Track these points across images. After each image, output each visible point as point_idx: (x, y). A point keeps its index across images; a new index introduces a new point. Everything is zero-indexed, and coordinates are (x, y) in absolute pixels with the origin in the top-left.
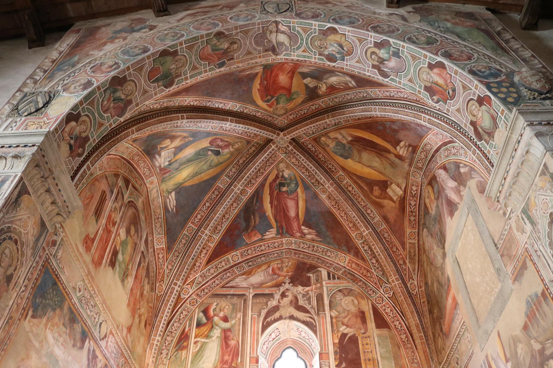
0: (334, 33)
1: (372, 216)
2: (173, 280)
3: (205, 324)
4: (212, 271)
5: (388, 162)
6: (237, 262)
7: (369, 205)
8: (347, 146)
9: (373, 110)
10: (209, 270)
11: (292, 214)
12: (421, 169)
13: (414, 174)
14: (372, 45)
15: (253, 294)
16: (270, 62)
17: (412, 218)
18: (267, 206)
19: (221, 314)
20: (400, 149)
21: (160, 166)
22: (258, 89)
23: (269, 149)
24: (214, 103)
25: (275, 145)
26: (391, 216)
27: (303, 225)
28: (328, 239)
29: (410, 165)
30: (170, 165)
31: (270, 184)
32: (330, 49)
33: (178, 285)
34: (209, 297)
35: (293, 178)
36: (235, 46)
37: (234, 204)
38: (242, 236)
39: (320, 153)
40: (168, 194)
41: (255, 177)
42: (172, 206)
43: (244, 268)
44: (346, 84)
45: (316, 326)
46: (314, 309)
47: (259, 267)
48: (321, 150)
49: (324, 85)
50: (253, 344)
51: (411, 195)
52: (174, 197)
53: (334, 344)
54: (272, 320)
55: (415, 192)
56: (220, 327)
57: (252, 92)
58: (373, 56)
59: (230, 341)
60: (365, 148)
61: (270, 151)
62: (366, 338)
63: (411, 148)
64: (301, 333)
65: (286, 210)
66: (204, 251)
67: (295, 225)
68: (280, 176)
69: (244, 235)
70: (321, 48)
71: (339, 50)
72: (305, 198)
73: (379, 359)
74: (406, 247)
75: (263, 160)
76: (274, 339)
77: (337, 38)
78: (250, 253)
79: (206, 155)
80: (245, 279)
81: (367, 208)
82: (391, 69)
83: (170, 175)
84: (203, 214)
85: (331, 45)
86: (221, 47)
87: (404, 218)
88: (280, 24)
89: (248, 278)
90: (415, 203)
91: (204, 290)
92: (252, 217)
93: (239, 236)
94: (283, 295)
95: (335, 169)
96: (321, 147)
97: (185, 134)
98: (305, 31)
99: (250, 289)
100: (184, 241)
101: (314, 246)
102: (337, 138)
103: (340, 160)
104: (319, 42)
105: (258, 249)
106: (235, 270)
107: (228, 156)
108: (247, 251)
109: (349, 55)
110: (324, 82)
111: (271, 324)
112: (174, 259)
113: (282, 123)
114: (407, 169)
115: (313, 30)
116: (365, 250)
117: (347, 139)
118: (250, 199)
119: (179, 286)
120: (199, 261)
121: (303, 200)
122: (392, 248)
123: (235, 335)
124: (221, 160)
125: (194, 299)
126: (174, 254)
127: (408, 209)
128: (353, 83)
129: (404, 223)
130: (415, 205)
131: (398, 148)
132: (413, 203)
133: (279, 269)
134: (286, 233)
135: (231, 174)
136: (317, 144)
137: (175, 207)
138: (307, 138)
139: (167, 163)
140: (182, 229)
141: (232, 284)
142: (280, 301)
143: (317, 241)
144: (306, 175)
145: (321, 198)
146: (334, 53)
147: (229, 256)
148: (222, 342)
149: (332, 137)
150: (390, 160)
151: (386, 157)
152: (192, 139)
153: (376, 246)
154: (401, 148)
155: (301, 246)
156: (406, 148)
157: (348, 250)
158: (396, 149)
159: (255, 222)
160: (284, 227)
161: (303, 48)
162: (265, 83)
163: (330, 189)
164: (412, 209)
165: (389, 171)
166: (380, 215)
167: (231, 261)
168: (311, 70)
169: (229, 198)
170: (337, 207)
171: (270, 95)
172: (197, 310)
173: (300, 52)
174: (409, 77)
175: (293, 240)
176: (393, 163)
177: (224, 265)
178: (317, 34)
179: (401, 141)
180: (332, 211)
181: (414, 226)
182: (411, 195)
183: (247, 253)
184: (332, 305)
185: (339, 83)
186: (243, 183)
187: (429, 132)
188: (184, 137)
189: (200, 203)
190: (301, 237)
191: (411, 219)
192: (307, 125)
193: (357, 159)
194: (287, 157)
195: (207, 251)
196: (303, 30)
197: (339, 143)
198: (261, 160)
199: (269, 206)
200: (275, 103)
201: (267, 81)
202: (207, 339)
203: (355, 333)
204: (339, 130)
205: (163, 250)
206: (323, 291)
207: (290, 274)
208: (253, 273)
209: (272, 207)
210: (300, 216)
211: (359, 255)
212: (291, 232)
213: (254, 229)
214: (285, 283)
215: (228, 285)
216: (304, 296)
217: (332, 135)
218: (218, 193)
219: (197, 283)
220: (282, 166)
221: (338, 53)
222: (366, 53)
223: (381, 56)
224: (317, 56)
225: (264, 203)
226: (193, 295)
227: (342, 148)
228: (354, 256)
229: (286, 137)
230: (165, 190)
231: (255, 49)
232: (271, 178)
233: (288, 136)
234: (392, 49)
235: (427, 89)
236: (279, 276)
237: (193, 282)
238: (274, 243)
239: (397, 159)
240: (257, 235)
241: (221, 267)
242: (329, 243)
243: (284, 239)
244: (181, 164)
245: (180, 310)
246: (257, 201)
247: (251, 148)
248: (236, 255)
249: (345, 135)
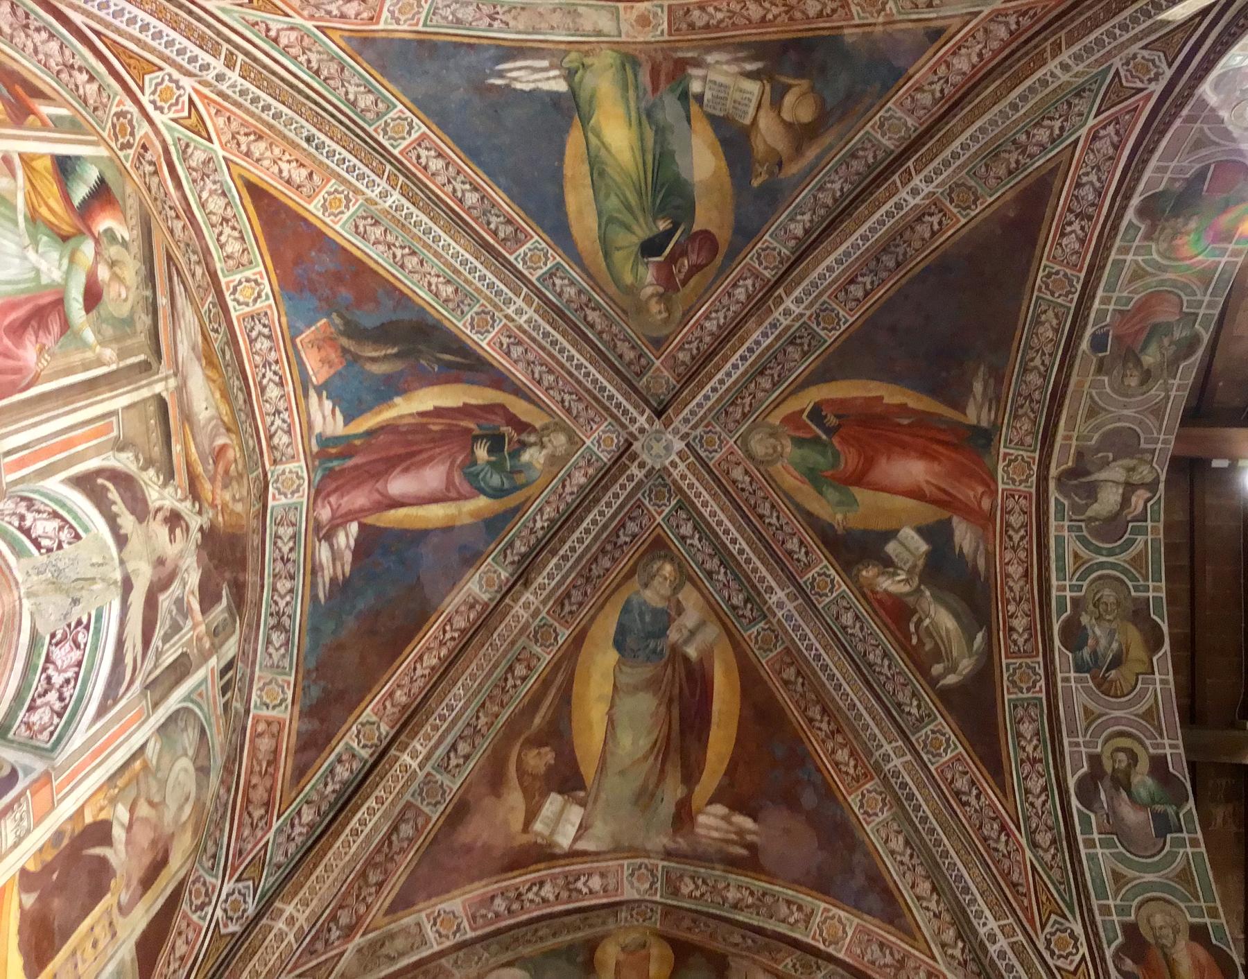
0: (1146, 642)
1: (453, 762)
2: (229, 41)
3: (67, 198)
4: (217, 204)
5: (646, 779)
6: (229, 299)
7: (484, 745)
8: (664, 645)
9: (894, 744)
10: (224, 194)
11: (398, 485)
12: (676, 892)
13: (643, 870)
14: (1151, 751)
15: (164, 394)
16: (1002, 450)
17: (500, 905)
18: (426, 400)
19: (103, 273)
20: (715, 816)
21: (698, 63)
22: (880, 398)
23: (636, 407)
24: (884, 275)
25: (647, 426)
26: (476, 831)
27: (362, 526)
28: (330, 625)
29: (668, 854)
30: (684, 96)
31: (502, 407)
32: (1098, 632)
33: (228, 73)
34: (141, 203)
35: (521, 479)
36: (1133, 382)
37: (450, 289)
38: (328, 316)
39: (614, 560)
40: (569, 69)
41: (531, 357)
42: (514, 74)
43: (216, 331)
44: (937, 656)
45: (116, 702)
46: (155, 667)
47: (226, 395)
48: (625, 563)
49: (906, 588)
50: (37, 457)
51: (571, 879)
52: (545, 86)
53: (80, 811)
54: (114, 508)
55: (585, 890)
56: (68, 273)
57: (873, 379)
58: (1122, 756)
59: (33, 338)
60: (671, 701)
61: (631, 409)
62: (111, 924)
63: (742, 852)
64: (68, 645)
65: (408, 462)
66: (299, 175)
67: (359, 499)
68: (524, 437)
69: (331, 323)
70: (1094, 605)
71: (1104, 656)
72: (458, 523)
74: (400, 914)
75: (603, 389)
76: (27, 532)
77: (1137, 651)
78: (258, 345)
79: (659, 212)
80: (193, 349)
81: (472, 737)
82: (1114, 812)
83: (637, 88)
84: (441, 179)
85: (1111, 634)
86: (1153, 348)
87: (491, 874)
88: (1148, 495)
89: (199, 359)
90: (552, 897)
91: (156, 173)
92: (390, 351)
93: (329, 306)
94: (174, 519)
95: (571, 612)
96: (636, 564)
97: (793, 169)
98: (1137, 561)
99: (175, 375)
100: (365, 101)
101: (292, 577)
102: (680, 610)
103: (607, 625)
104: (1112, 599)
105: (269, 374)
106: (210, 299)
107: (628, 279)
108: (269, 337)
109: (1099, 686)
110: (917, 590)
111: (101, 512)
112: (314, 57)
113: (711, 443)
114: (649, 846)
115: (1142, 582)
116: (332, 771)
117: (687, 641)
118: (457, 339)
119: (220, 78)
120: (268, 154)
121: (453, 517)
122: (376, 866)
123: (52, 355)
124: (618, 256)
125: (132, 134)
126: (332, 59)
127: (521, 880)
128: (951, 679)
129: (472, 881)
130: (544, 900)
131: (720, 809)
132: (548, 891)
133: (227, 472)
134: (325, 469)
135: (558, 282)
136: (646, 551)
137: (508, 86)
138: (659, 519)
139: (696, 87)
140: (414, 101)
141: (181, 300)
142: (160, 516)
143: (314, 585)
144: (535, 521)
145: (467, 576)
146: (1090, 642)
147: (262, 268)
148: (27, 300)
149: (680, 596)
150: (657, 786)
151: (662, 771)
152: (756, 183)
153: (378, 815)
154: (725, 818)
155: (281, 531)
156: (734, 837)
157: (311, 706)
158: (710, 802)
159: (374, 360)
160: (350, 463)
161: (1084, 553)
162: (906, 422)
163: (521, 612)
164: (531, 895)
165: (617, 788)
166: (467, 787)
167: (237, 277)
168: (969, 559)
169: (494, 279)
170: (448, 636)
171: (840, 426)
172: (103, 152)
173: (1072, 545)
174: (1121, 868)
175: (302, 498)
176: (653, 795)
177: (229, 249)
178: (1133, 594)
179: (755, 820)
180: (433, 619)
181: (480, 921)
182: (571, 879)
183: (260, 333)
184: (171, 727)
185: (931, 635)
186: (537, 328)
187: (866, 917)
188: (780, 164)
189: (485, 172)
190: (318, 527)
191: (498, 901)
192: (739, 529)
193: (624, 679)
194: (588, 456)
195: (299, 187)
196: (1139, 554)
197: (663, 619)
198: (606, 383)
199: (428, 405)
200: (800, 434)
201: (909, 426)
202: (25, 216)
203: (119, 872)
204: (714, 617)
205: (371, 19)
206: (198, 668)
207: (220, 519)
208: (210, 373)
209: (422, 414)
210: (392, 512)
211: (310, 753)
212: (334, 485)
213: (349, 357)
214: (200, 513)
215: (175, 278)
216: (179, 602)
217: (689, 598)
218: (502, 235)
219: (187, 145)
220: (560, 440)
221: (1094, 653)
222: (1121, 734)
223: (1135, 780)
224: (1068, 594)
225: (436, 389)
226: (146, 127)
227: (650, 629)
228: (299, 734)
229: (678, 460)
230: (588, 61)
231: (1097, 428)
232: (519, 408)
233: (682, 466)
234: (1171, 810)
235: (1131, 930)
236: (212, 480)
237: (200, 129)
238: (289, 432)
239: (673, 810)
240: (326, 367)
241: (223, 239)
242: (315, 630)
243: (303, 463)
244: (661, 132)
245: (101, 68)
246: (449, 365)
247: (633, 348)
248: (259, 296)
249: (699, 638)
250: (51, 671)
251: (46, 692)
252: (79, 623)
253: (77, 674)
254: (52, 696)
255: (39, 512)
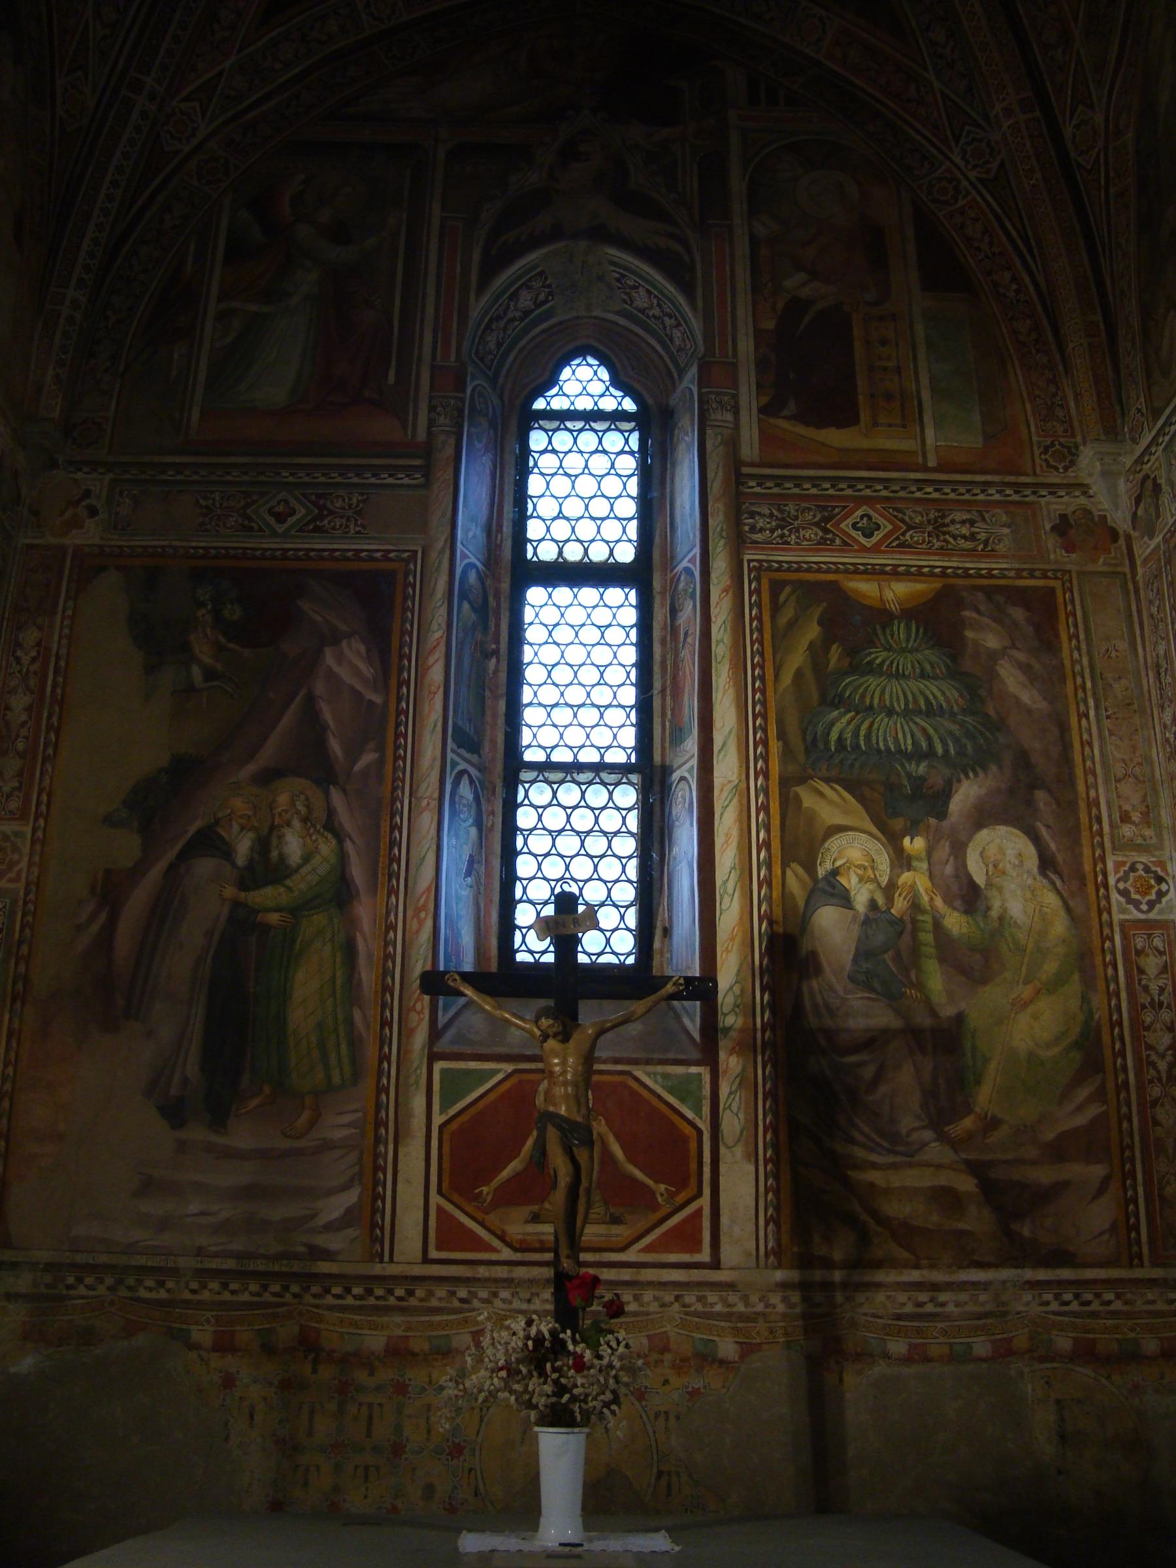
53: (758, 334)
73: (926, 396)
250: (651, 313)
251: (663, 323)
252: (618, 280)
253: (655, 296)
254: (668, 322)
255: (508, 307)
